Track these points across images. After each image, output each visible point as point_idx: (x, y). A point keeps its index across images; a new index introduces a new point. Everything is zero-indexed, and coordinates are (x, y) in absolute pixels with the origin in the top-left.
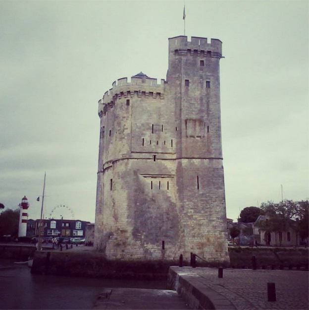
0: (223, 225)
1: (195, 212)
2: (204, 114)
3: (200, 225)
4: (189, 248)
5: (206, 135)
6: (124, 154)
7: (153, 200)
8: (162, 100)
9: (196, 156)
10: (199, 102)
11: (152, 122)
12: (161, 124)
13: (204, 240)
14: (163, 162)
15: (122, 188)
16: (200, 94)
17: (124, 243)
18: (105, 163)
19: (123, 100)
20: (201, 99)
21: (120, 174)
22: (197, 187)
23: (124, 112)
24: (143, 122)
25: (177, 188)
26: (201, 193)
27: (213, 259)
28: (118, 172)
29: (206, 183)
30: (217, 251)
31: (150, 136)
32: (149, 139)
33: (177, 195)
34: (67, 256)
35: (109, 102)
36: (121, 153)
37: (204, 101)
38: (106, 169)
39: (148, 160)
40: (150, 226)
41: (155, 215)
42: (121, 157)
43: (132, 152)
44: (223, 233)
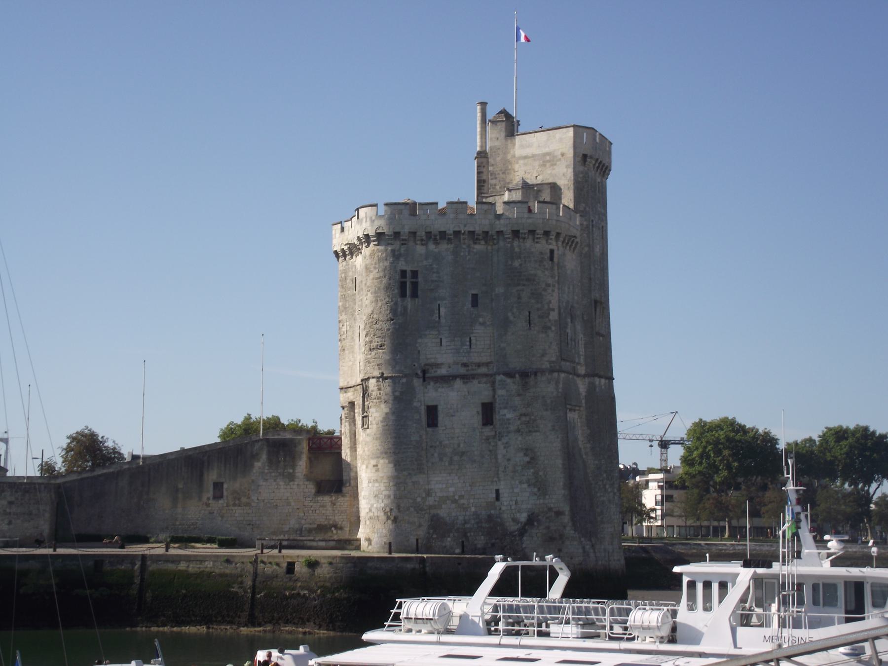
6: (553, 362)
15: (554, 429)
17: (561, 536)
18: (456, 363)
19: (543, 246)
21: (549, 401)
23: (546, 273)
25: (589, 431)
28: (543, 397)
33: (588, 445)
34: (459, 564)
35: (478, 229)
36: (546, 359)
38: (454, 377)
42: (546, 365)
43: (562, 359)
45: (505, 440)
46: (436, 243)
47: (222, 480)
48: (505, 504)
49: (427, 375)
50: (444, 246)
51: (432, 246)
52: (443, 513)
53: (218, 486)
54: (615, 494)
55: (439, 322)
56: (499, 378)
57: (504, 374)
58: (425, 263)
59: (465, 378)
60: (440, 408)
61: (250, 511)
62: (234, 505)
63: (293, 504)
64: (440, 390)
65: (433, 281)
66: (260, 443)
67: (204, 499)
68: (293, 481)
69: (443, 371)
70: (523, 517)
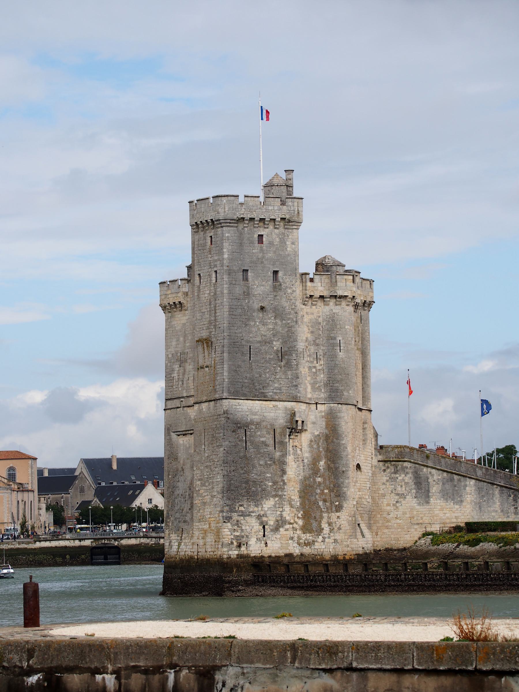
0: (221, 503)
1: (203, 485)
2: (212, 327)
3: (205, 504)
4: (196, 538)
5: (213, 362)
7: (183, 470)
8: (187, 312)
9: (204, 399)
10: (208, 309)
11: (179, 350)
12: (186, 351)
13: (206, 527)
14: (188, 409)
16: (209, 294)
20: (210, 305)
22: (203, 447)
24: (172, 350)
26: (207, 455)
27: (212, 553)
29: (210, 439)
30: (215, 541)
31: (178, 373)
32: (177, 377)
37: (212, 306)
39: (178, 410)
40: (176, 508)
41: (181, 493)
44: (221, 514)
54: (213, 497)
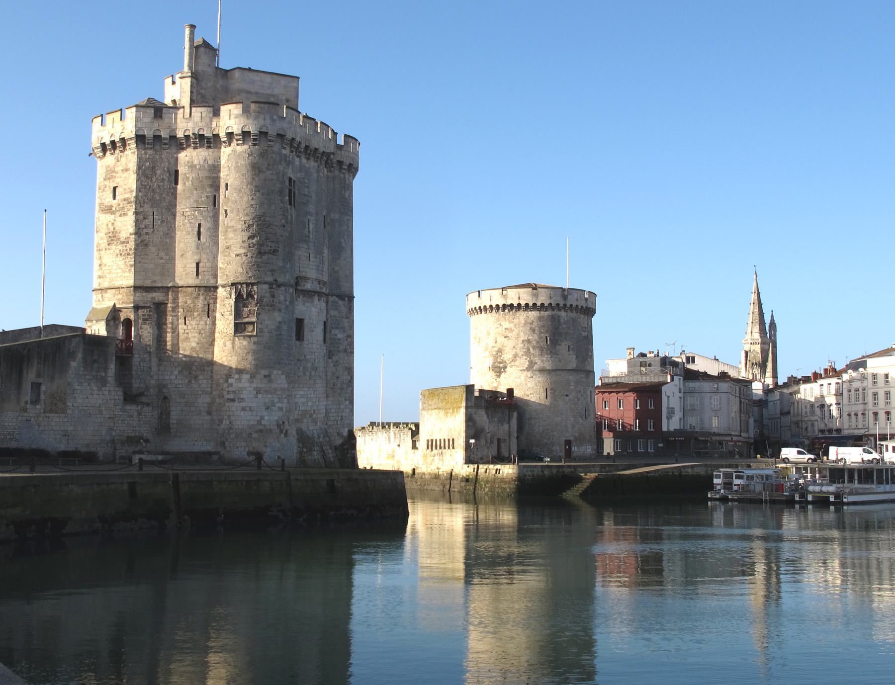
38: (315, 292)
45: (335, 358)
46: (308, 159)
47: (40, 380)
48: (332, 419)
49: (299, 288)
50: (312, 164)
51: (304, 161)
52: (304, 428)
53: (36, 386)
55: (309, 237)
56: (331, 299)
57: (337, 296)
58: (299, 175)
59: (320, 294)
60: (306, 322)
61: (66, 420)
62: (51, 411)
63: (104, 412)
64: (307, 304)
65: (305, 195)
66: (77, 339)
67: (23, 404)
68: (105, 386)
69: (308, 286)
70: (345, 433)
